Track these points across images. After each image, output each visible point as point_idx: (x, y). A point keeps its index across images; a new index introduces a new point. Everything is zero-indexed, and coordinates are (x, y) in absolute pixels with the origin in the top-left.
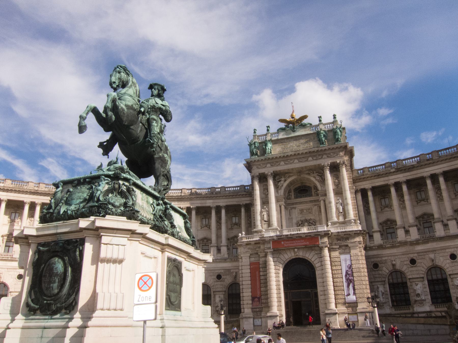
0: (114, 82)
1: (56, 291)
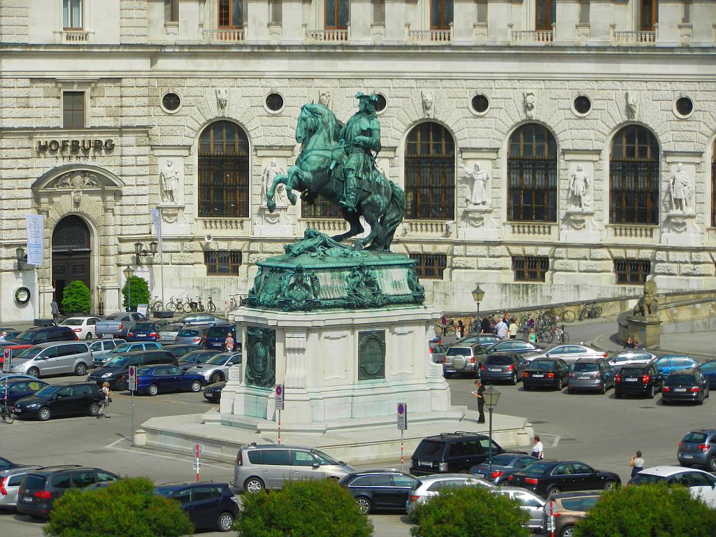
0: (300, 137)
1: (262, 369)
